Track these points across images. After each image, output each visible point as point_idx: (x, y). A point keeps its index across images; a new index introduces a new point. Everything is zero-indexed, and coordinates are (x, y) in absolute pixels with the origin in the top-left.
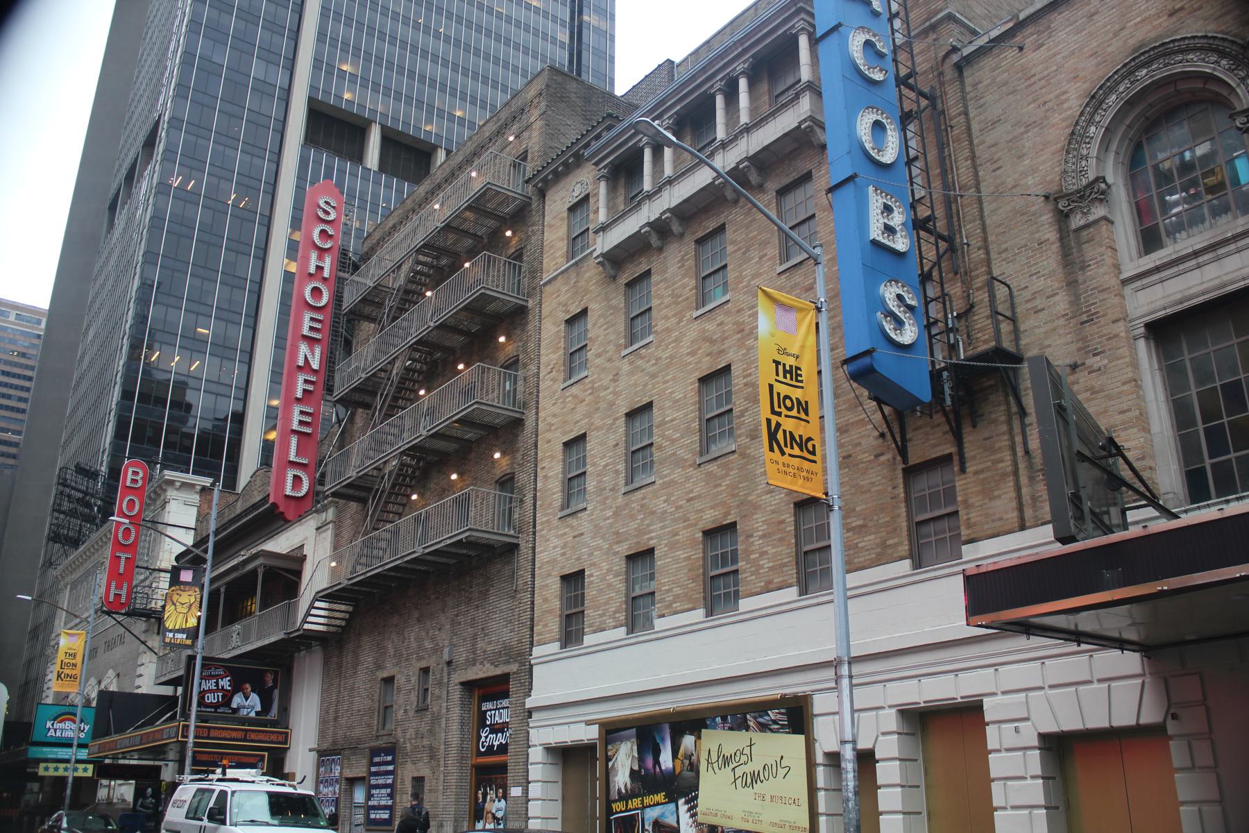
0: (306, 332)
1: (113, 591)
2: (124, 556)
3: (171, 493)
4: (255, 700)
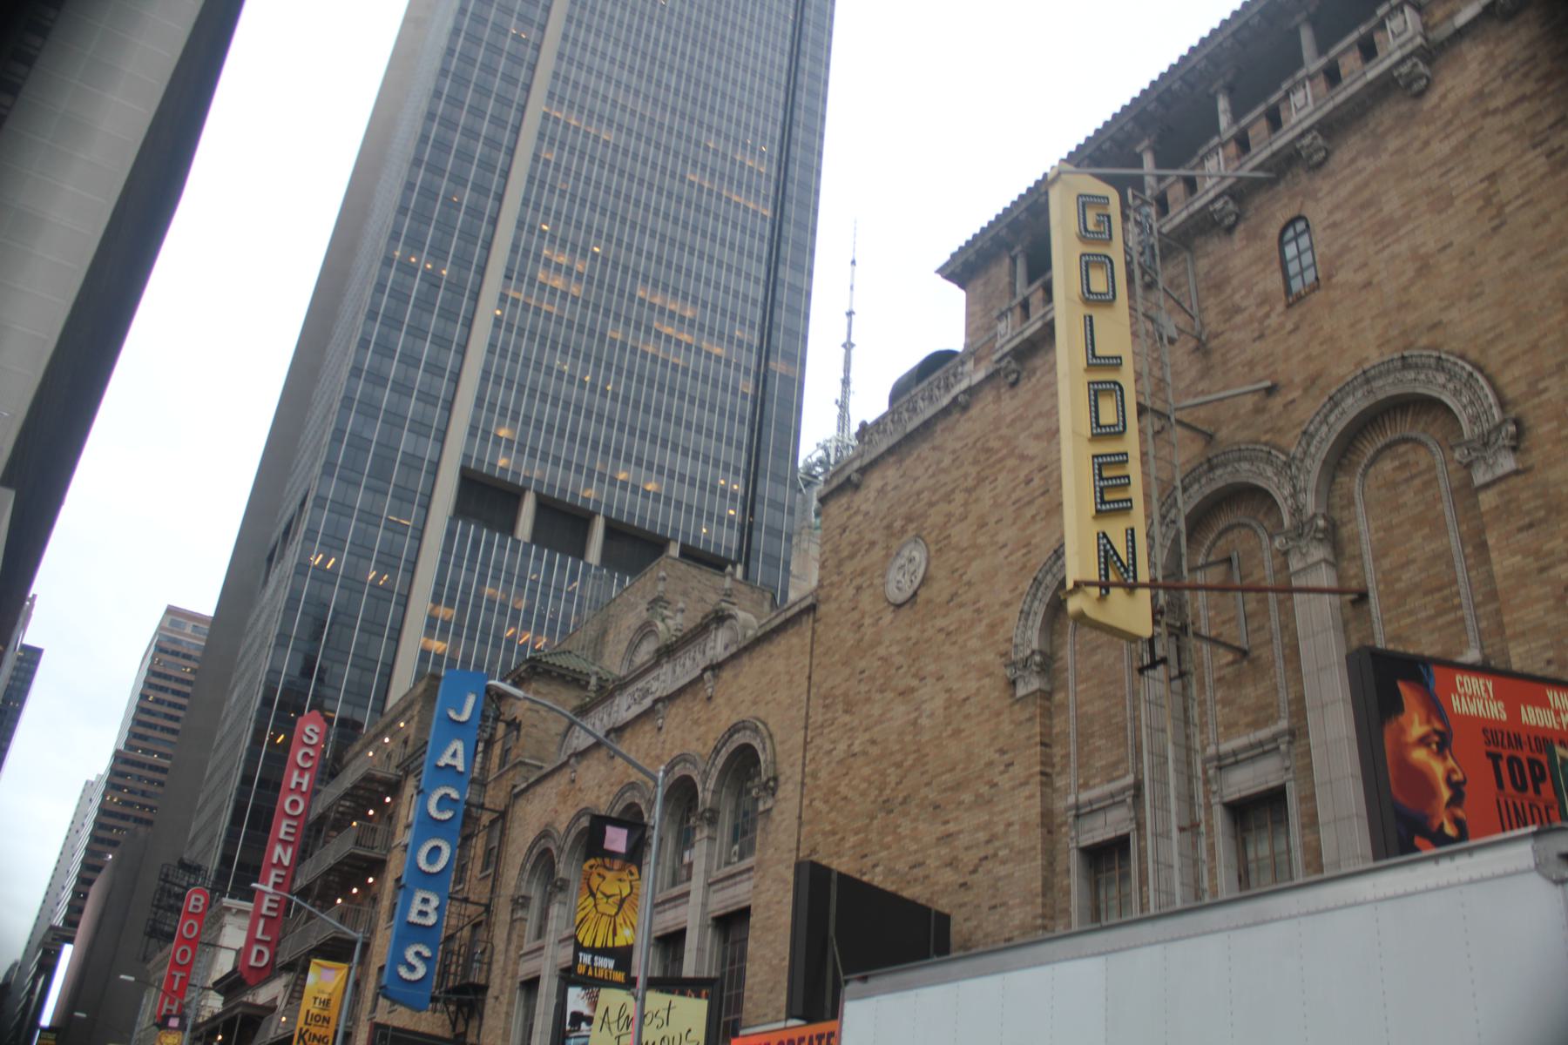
0: (282, 836)
1: (166, 1006)
2: (179, 975)
3: (228, 918)
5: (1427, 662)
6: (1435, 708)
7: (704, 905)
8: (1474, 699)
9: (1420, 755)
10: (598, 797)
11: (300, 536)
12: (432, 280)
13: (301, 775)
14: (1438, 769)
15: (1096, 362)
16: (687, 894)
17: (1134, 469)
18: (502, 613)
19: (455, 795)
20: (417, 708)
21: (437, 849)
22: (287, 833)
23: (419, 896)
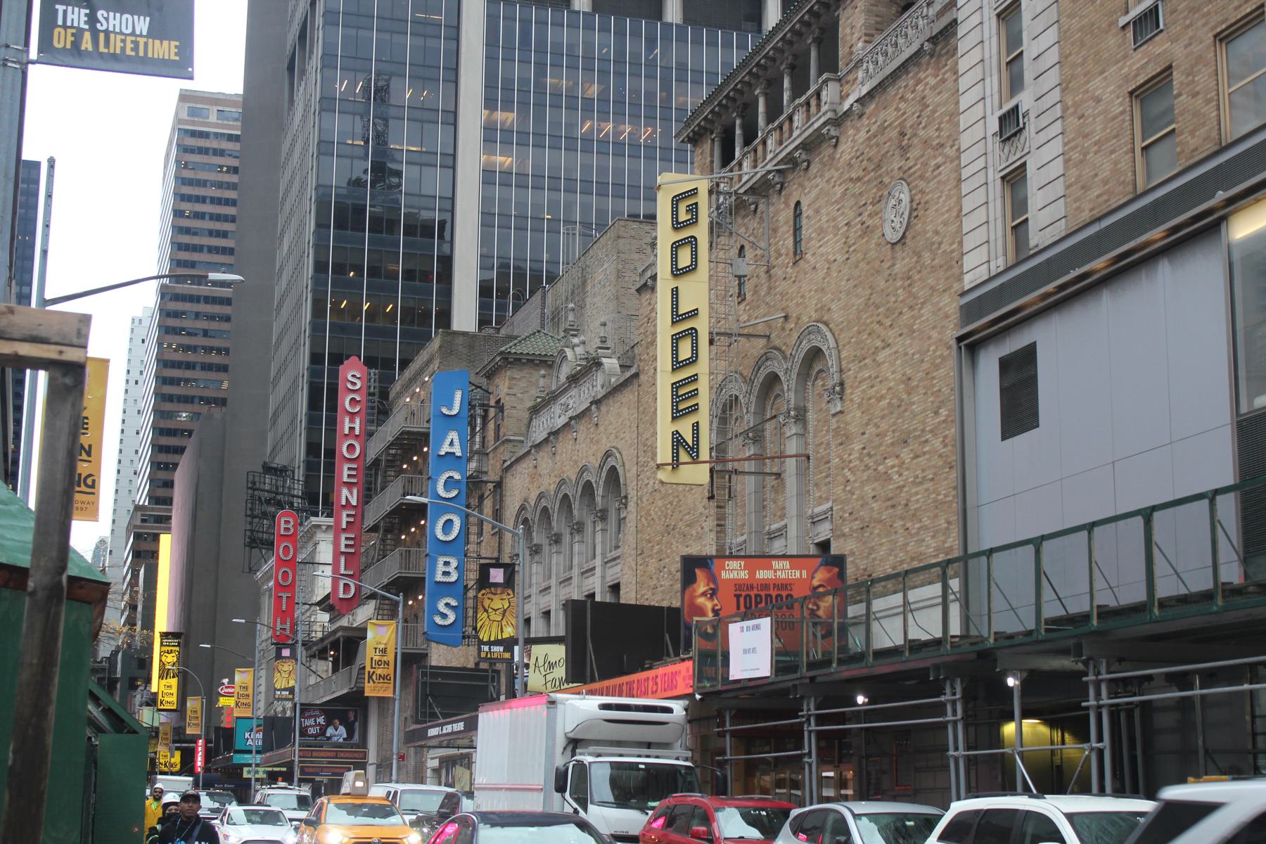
0: (345, 479)
1: (279, 626)
4: (342, 730)
5: (711, 558)
6: (712, 578)
7: (603, 577)
8: (733, 571)
9: (701, 600)
11: (315, 62)
13: (352, 421)
15: (677, 318)
16: (594, 568)
17: (703, 386)
19: (457, 476)
20: (436, 363)
21: (449, 522)
22: (349, 476)
23: (441, 560)
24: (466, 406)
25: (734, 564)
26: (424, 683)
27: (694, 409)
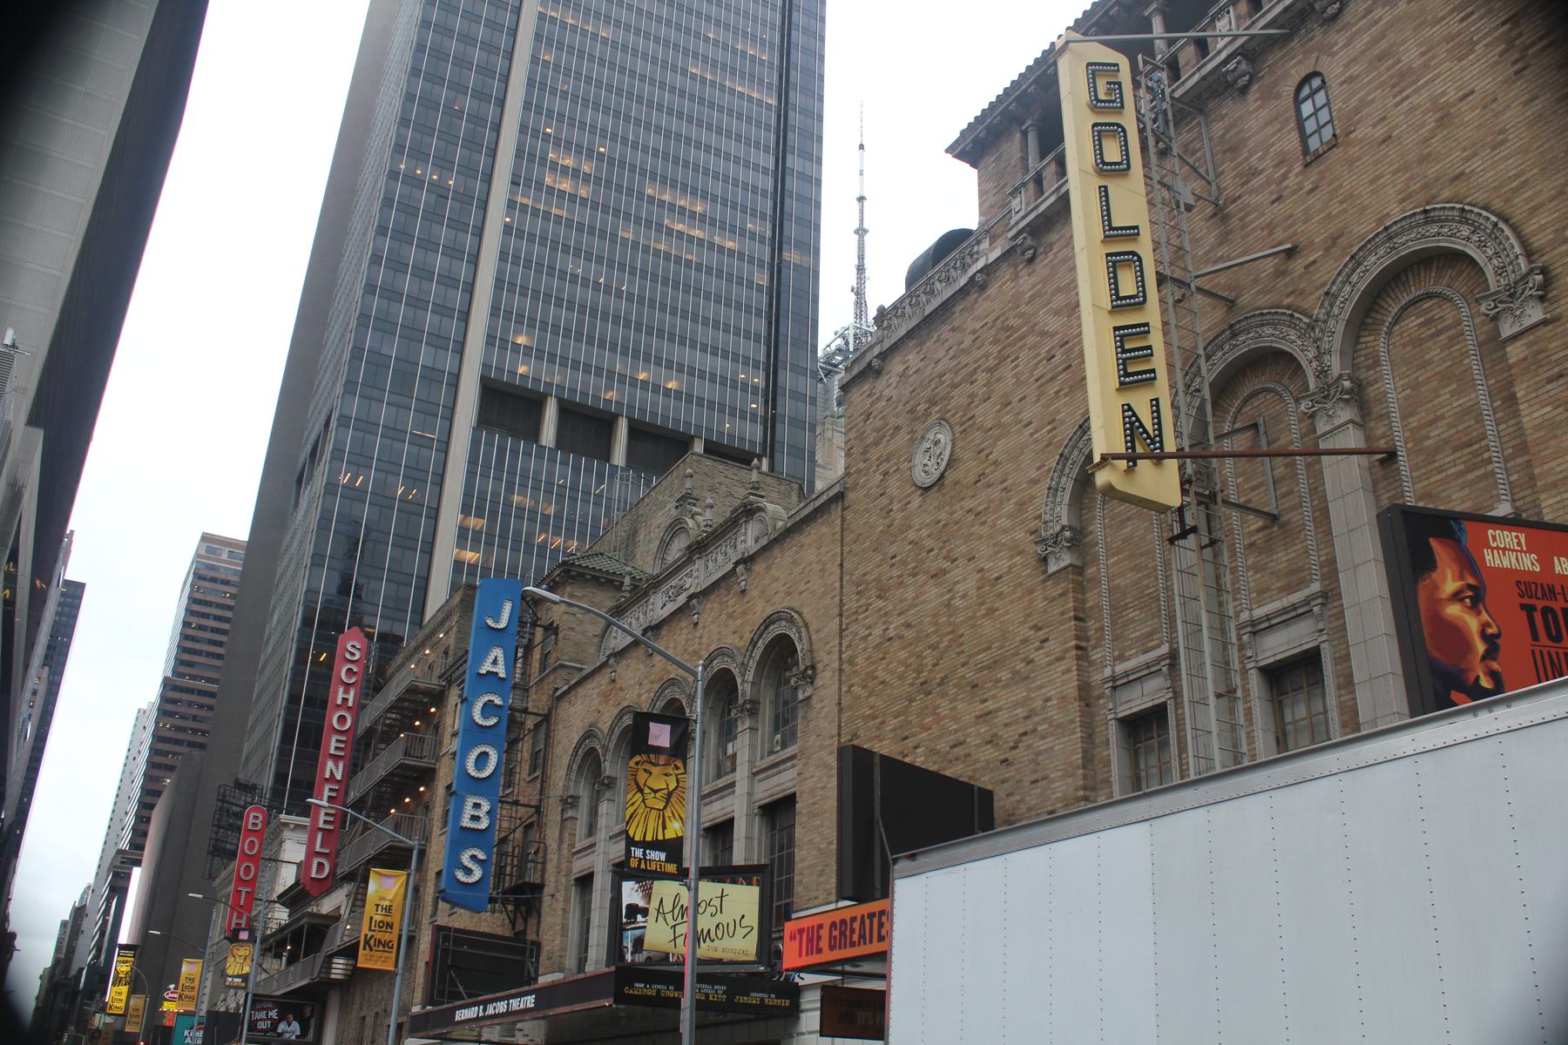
0: (332, 751)
1: (235, 920)
3: (287, 834)
4: (296, 1026)
5: (1459, 517)
6: (1468, 563)
7: (750, 794)
8: (1506, 553)
9: (1453, 610)
10: (640, 695)
11: (327, 456)
12: (440, 193)
13: (346, 692)
14: (1472, 623)
15: (1113, 232)
16: (733, 784)
17: (1156, 340)
18: (532, 520)
19: (498, 701)
20: (455, 618)
21: (484, 755)
22: (337, 748)
23: (470, 801)
24: (516, 623)
25: (1506, 538)
26: (445, 951)
27: (1148, 378)
